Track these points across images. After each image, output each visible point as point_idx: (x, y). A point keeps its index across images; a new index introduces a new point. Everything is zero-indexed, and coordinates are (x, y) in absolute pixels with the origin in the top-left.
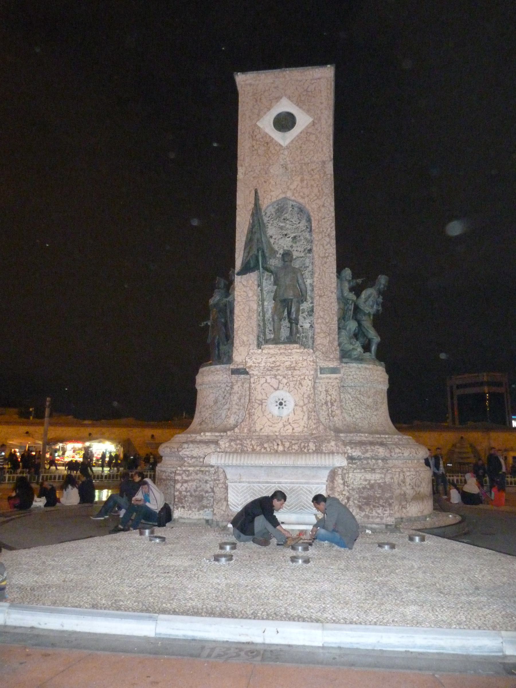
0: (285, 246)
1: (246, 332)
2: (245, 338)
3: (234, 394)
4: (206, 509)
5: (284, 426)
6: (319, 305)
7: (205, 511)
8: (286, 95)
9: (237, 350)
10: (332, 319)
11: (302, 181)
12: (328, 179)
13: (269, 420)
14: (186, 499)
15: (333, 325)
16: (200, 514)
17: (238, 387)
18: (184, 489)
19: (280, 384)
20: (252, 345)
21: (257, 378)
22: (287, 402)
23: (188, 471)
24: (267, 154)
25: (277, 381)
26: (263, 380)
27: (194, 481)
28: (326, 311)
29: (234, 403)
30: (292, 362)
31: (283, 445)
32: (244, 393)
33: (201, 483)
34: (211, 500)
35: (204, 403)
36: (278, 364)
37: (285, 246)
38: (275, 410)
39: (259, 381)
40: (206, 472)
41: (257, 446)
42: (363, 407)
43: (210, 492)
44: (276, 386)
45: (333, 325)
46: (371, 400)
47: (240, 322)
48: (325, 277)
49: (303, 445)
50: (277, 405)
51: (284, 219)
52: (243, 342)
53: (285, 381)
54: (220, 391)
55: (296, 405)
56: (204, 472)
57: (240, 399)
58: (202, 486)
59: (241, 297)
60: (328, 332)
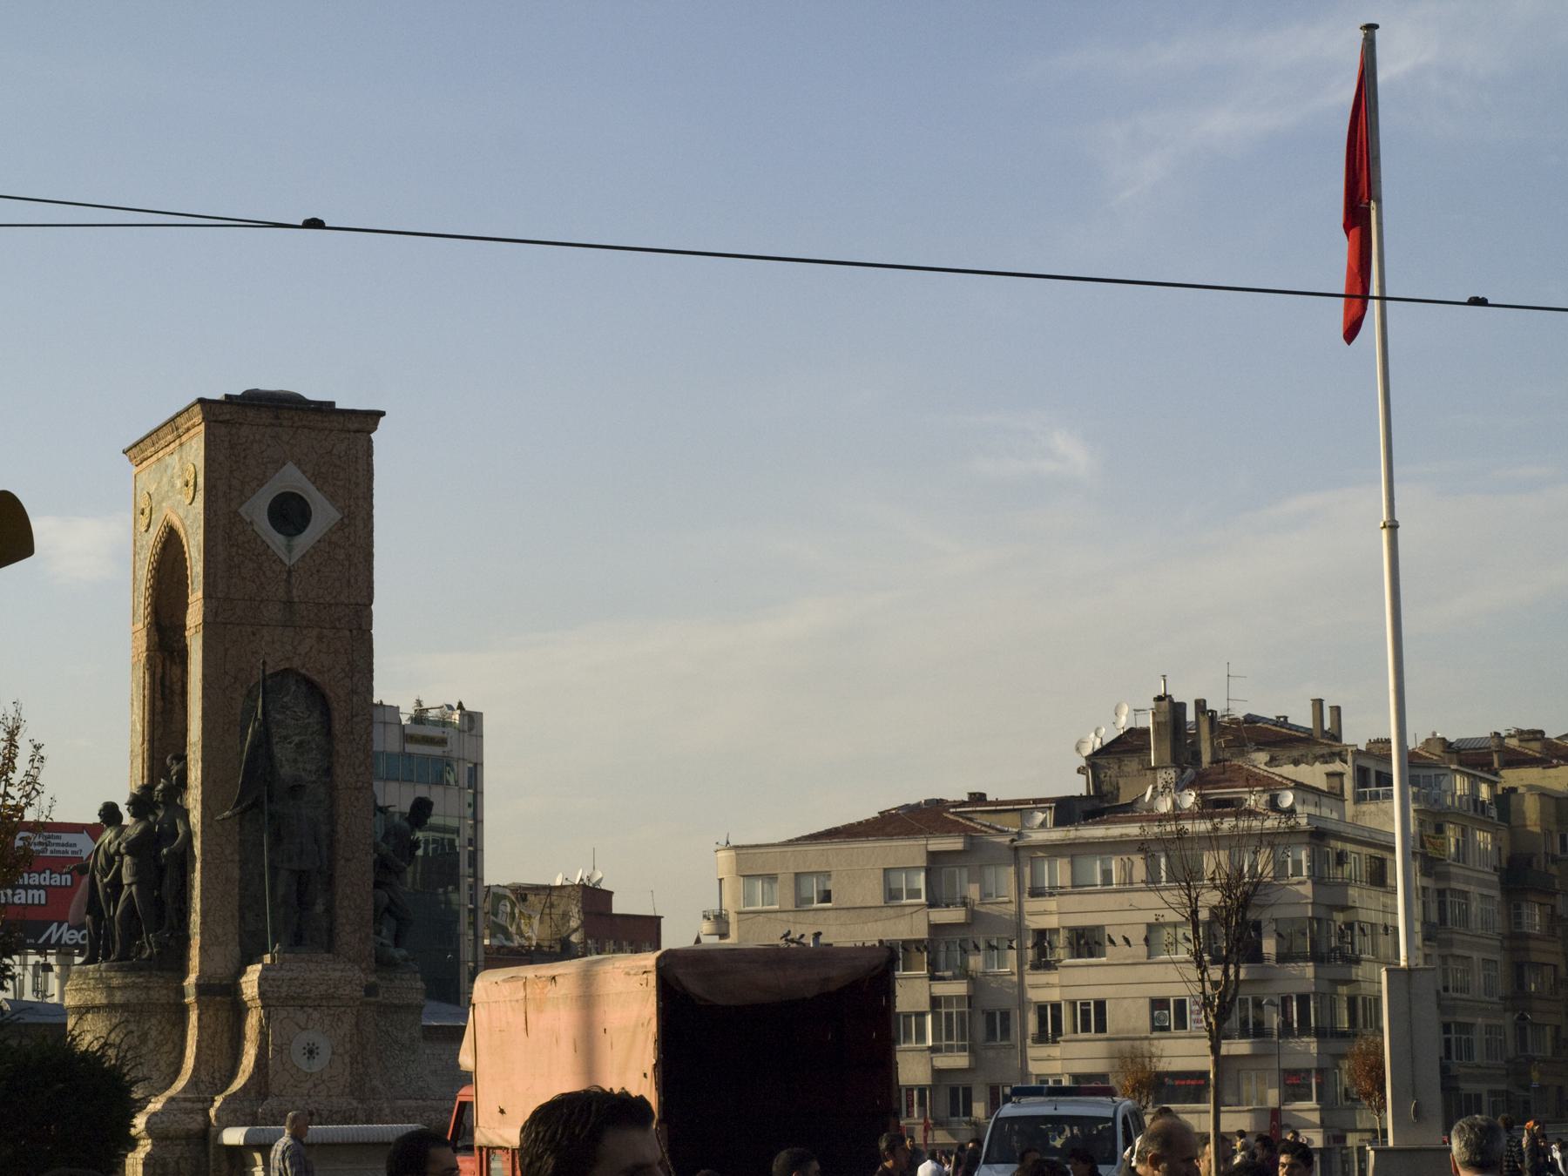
0: (284, 759)
1: (221, 918)
5: (315, 1086)
11: (320, 638)
36: (308, 988)
37: (284, 759)
38: (302, 1061)
42: (396, 1047)
46: (406, 1035)
51: (282, 707)
53: (316, 1015)
55: (333, 1053)
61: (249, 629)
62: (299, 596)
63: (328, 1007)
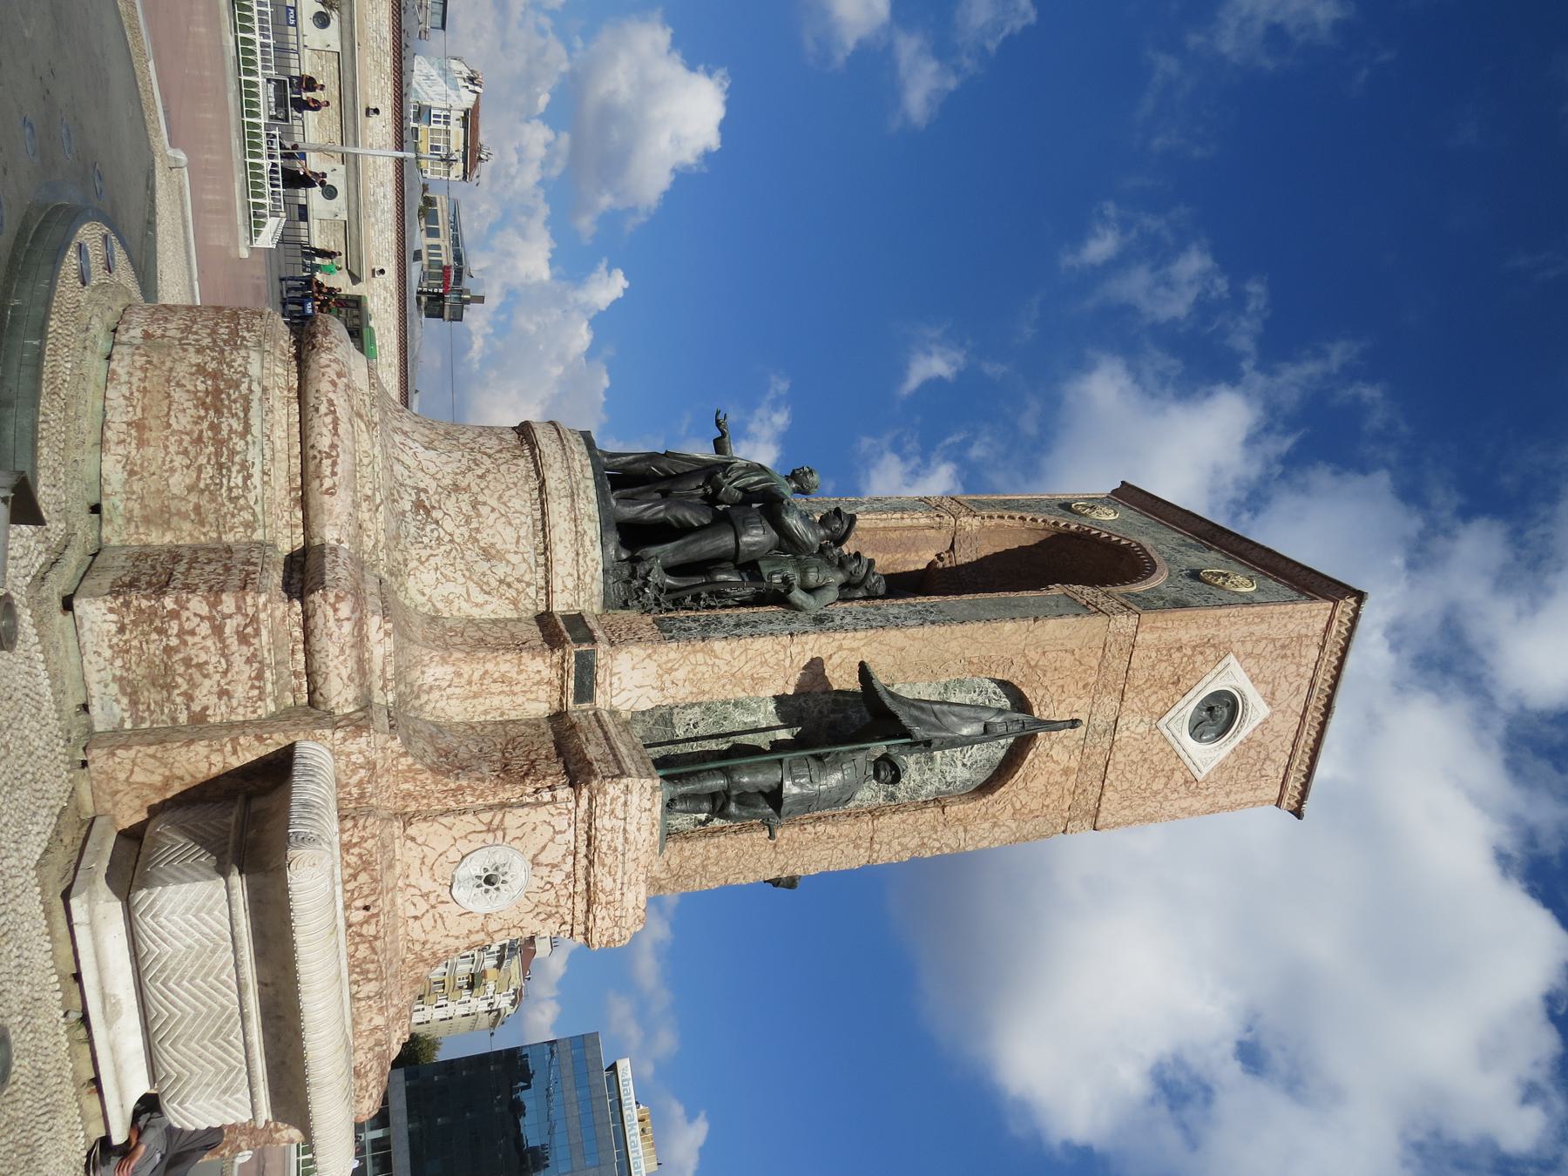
2: (680, 675)
3: (516, 661)
4: (125, 701)
5: (425, 896)
6: (753, 845)
7: (117, 701)
8: (1272, 714)
9: (649, 656)
10: (713, 878)
11: (1066, 772)
12: (1056, 828)
13: (441, 855)
14: (154, 636)
15: (698, 881)
16: (106, 686)
17: (539, 672)
18: (187, 626)
19: (549, 868)
20: (660, 694)
21: (567, 808)
22: (496, 893)
23: (257, 633)
24: (1151, 685)
25: (560, 858)
26: (561, 823)
27: (223, 655)
28: (735, 862)
29: (490, 666)
30: (612, 892)
31: (367, 921)
32: (517, 689)
33: (217, 677)
34: (162, 713)
35: (485, 504)
36: (608, 861)
39: (560, 814)
40: (259, 688)
41: (360, 856)
43: (188, 708)
44: (542, 858)
45: (698, 881)
47: (728, 657)
48: (822, 850)
49: (372, 967)
50: (486, 870)
52: (670, 671)
53: (558, 878)
54: (524, 566)
56: (257, 684)
57: (503, 680)
58: (207, 683)
59: (799, 653)
60: (681, 873)
61: (1091, 680)
62: (1120, 740)
63: (572, 896)
